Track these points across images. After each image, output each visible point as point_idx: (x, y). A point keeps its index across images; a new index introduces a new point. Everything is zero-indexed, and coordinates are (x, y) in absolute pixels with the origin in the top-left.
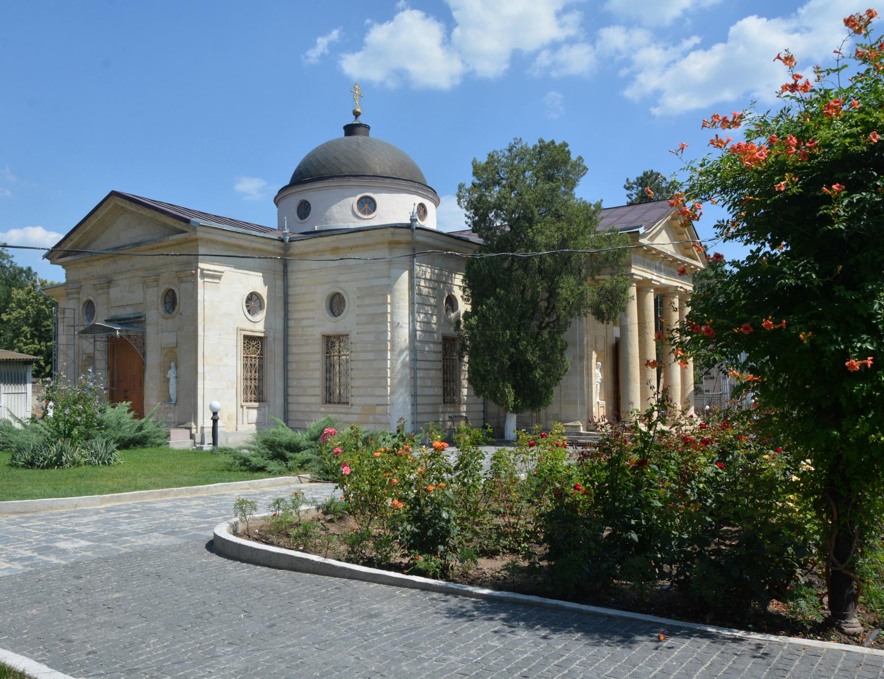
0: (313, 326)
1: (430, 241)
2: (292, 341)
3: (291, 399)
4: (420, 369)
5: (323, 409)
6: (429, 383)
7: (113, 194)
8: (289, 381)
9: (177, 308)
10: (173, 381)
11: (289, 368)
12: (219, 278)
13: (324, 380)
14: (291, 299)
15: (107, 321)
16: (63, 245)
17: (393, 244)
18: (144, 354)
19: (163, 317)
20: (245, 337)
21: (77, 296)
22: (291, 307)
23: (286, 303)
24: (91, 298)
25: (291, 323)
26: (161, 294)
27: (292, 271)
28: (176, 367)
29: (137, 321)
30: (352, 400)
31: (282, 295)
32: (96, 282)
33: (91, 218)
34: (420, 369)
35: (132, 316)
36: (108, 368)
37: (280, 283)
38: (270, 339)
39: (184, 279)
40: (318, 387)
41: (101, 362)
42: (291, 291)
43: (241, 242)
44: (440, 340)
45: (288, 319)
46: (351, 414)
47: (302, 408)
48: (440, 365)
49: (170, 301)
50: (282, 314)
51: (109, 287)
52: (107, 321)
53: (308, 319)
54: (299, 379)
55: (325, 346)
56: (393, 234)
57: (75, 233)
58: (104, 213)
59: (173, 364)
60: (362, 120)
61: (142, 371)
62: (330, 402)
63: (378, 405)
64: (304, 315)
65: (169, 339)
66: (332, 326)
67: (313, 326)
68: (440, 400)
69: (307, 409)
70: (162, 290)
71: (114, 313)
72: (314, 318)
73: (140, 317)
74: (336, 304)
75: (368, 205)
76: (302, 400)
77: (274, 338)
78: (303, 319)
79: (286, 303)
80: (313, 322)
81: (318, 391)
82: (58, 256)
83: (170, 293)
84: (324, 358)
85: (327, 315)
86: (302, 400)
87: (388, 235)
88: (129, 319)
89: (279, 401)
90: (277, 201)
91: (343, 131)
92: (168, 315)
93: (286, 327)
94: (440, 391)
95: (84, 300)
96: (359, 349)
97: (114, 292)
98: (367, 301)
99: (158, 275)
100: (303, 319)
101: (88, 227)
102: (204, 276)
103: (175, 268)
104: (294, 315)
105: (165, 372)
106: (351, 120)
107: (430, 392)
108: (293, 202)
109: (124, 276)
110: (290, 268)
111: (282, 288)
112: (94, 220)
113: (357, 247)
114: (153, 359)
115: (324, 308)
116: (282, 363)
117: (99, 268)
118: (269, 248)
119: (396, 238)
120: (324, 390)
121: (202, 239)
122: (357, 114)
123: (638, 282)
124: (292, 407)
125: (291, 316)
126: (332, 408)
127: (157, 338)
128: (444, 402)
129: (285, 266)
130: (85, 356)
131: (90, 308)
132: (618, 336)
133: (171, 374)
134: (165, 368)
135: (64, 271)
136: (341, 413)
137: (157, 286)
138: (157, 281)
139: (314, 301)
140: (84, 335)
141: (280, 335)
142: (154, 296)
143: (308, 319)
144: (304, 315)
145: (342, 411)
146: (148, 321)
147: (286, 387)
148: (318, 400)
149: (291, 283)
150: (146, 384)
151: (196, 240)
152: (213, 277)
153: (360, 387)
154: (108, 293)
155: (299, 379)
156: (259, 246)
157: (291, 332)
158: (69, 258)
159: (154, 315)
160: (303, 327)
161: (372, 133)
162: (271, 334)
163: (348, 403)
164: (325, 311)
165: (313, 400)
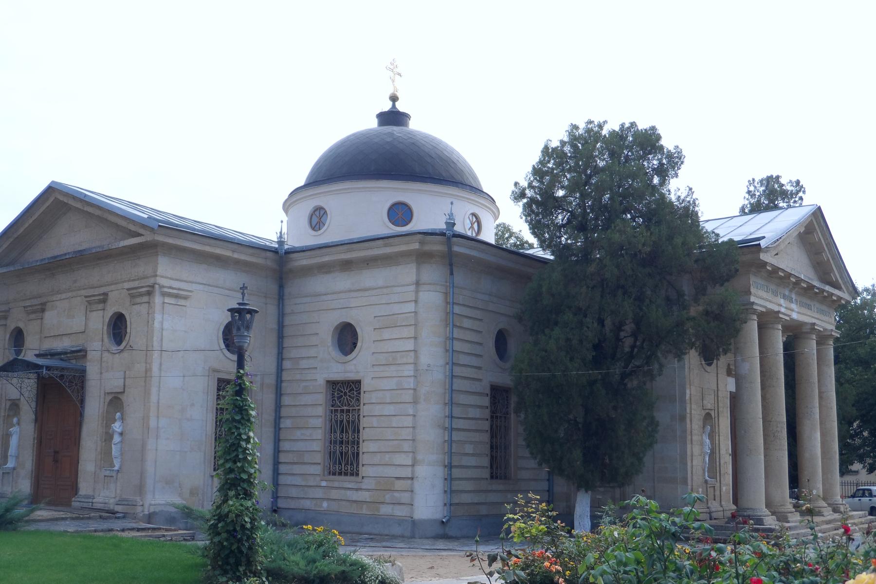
1: (474, 253)
3: (283, 469)
4: (458, 430)
5: (324, 484)
6: (469, 449)
8: (282, 444)
10: (116, 438)
12: (185, 298)
13: (327, 444)
14: (287, 331)
15: (37, 356)
22: (287, 343)
23: (281, 337)
24: (21, 325)
25: (287, 364)
26: (107, 320)
30: (363, 471)
31: (275, 326)
34: (458, 430)
36: (36, 420)
41: (28, 412)
42: (288, 321)
43: (218, 251)
44: (488, 391)
47: (298, 481)
48: (486, 425)
50: (275, 351)
51: (43, 311)
52: (37, 356)
55: (329, 397)
56: (422, 243)
60: (401, 107)
62: (334, 474)
65: (114, 382)
66: (341, 369)
68: (486, 474)
69: (303, 483)
70: (109, 313)
74: (347, 338)
75: (400, 213)
77: (262, 385)
79: (281, 337)
81: (318, 458)
85: (335, 353)
86: (297, 469)
88: (66, 353)
90: (287, 206)
93: (280, 370)
94: (486, 461)
95: (13, 327)
98: (387, 334)
102: (164, 294)
104: (290, 354)
106: (387, 106)
107: (472, 461)
108: (306, 207)
109: (64, 296)
110: (287, 290)
114: (94, 407)
115: (330, 344)
118: (260, 261)
119: (427, 248)
120: (327, 456)
121: (164, 244)
122: (394, 99)
123: (761, 315)
125: (286, 354)
128: (492, 477)
129: (281, 287)
130: (8, 403)
132: (734, 390)
138: (104, 301)
141: (271, 380)
142: (99, 321)
145: (350, 486)
148: (317, 470)
149: (288, 310)
152: (177, 296)
156: (243, 257)
157: (285, 376)
164: (331, 349)
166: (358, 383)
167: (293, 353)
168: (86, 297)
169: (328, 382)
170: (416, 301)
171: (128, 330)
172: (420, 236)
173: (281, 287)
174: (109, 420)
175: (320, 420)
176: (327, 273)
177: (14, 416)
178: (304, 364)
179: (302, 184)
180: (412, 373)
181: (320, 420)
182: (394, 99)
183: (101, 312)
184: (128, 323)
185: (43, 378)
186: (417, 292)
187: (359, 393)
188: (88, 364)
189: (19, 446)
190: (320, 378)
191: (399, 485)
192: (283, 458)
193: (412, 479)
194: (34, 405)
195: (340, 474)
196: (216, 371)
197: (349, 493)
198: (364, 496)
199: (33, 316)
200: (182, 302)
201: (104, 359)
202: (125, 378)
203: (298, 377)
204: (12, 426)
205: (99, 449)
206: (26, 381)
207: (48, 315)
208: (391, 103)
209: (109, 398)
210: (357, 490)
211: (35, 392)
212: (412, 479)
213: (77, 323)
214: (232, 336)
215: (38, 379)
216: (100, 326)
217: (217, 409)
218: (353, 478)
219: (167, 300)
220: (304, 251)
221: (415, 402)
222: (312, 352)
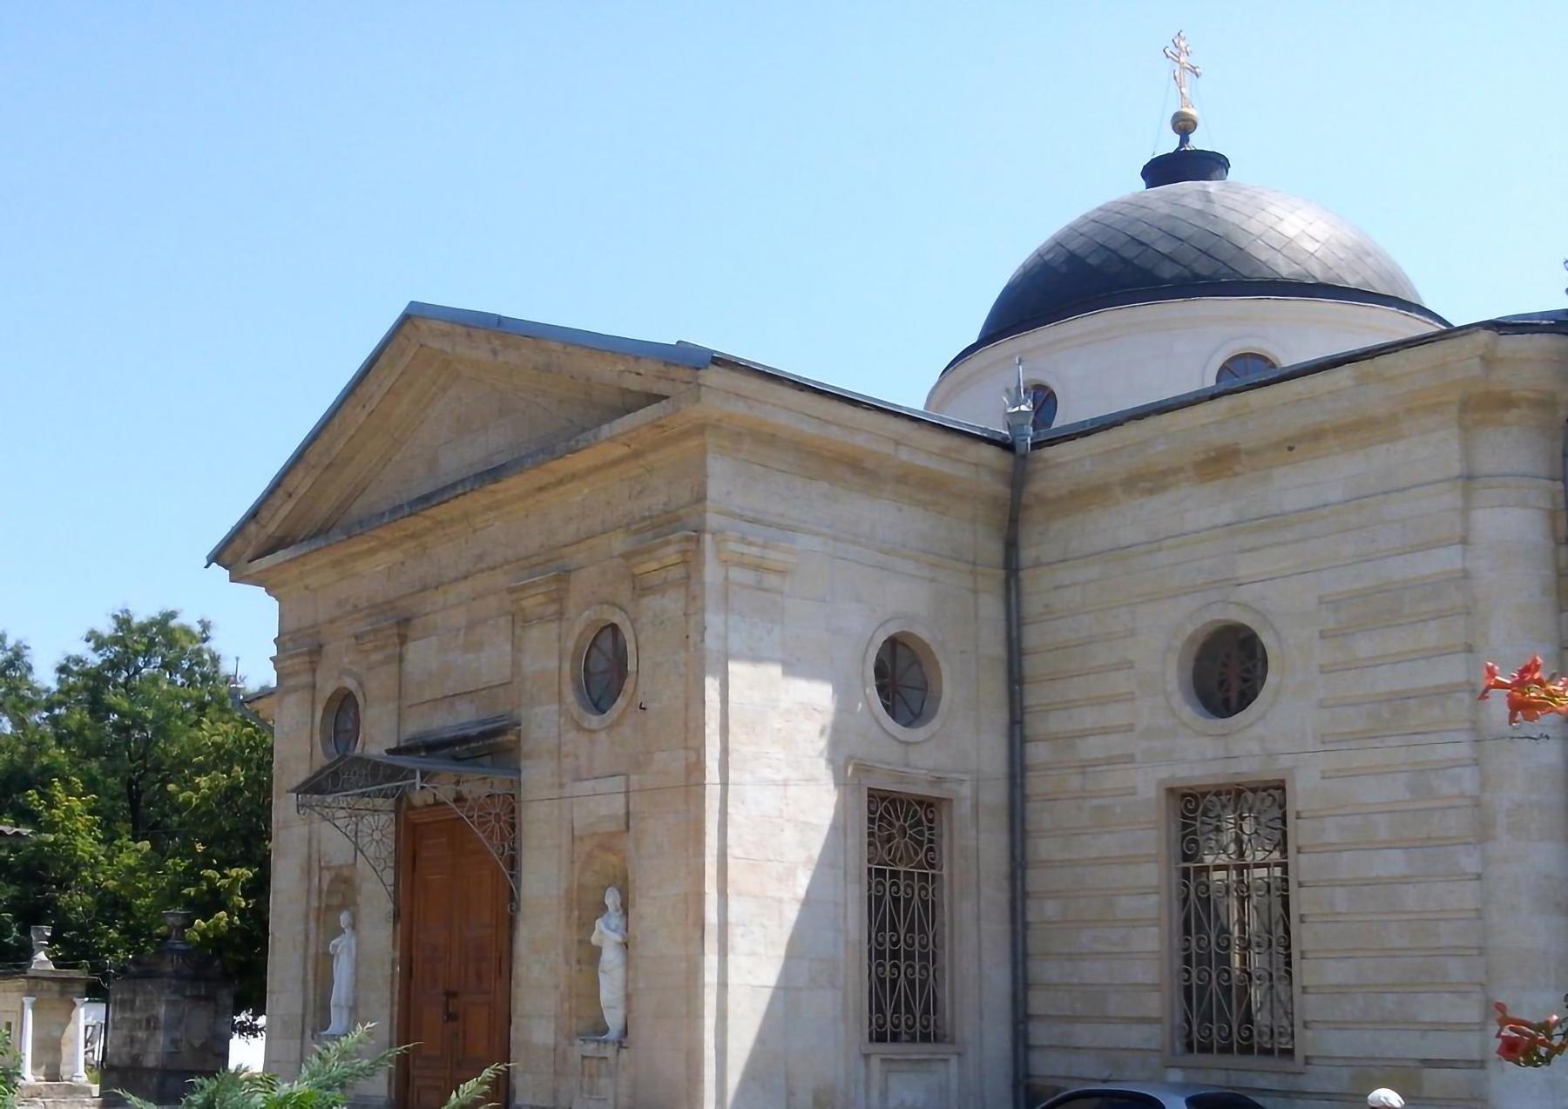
0: (1131, 758)
2: (1039, 816)
9: (629, 685)
11: (1031, 917)
13: (1178, 963)
14: (1032, 665)
17: (1482, 407)
19: (579, 728)
22: (1034, 696)
23: (1015, 679)
24: (350, 684)
25: (1037, 753)
26: (570, 644)
27: (1037, 564)
28: (625, 907)
29: (489, 746)
31: (998, 650)
32: (363, 627)
37: (992, 607)
38: (963, 809)
40: (1156, 987)
41: (376, 896)
42: (1032, 637)
45: (1024, 740)
50: (1002, 717)
51: (403, 640)
52: (389, 752)
53: (1105, 731)
54: (1070, 957)
55: (1176, 833)
59: (612, 899)
61: (509, 924)
62: (1206, 1049)
64: (1088, 718)
65: (600, 804)
66: (1208, 751)
67: (1131, 758)
71: (415, 726)
72: (1130, 728)
73: (501, 731)
77: (976, 807)
78: (1085, 734)
79: (1015, 679)
81: (1153, 1004)
83: (606, 643)
84: (1176, 877)
88: (465, 740)
96: (1332, 836)
97: (421, 655)
99: (564, 575)
100: (1085, 734)
104: (1046, 725)
105: (587, 926)
110: (1027, 554)
111: (1002, 625)
113: (1316, 435)
114: (543, 879)
116: (1003, 898)
125: (1033, 725)
127: (561, 804)
129: (1011, 546)
130: (327, 876)
131: (343, 712)
133: (606, 934)
137: (560, 616)
138: (559, 598)
139: (1130, 665)
143: (1105, 731)
144: (1088, 718)
146: (526, 747)
147: (1021, 986)
149: (1032, 605)
151: (700, 429)
153: (1341, 990)
154: (401, 659)
155: (1070, 957)
157: (1036, 784)
158: (281, 556)
159: (546, 722)
160: (1084, 767)
162: (966, 790)
163: (1288, 1053)
164: (1177, 699)
165: (1135, 1036)
167: (1055, 723)
169: (1171, 791)
170: (1464, 541)
171: (631, 667)
172: (1485, 336)
173: (1011, 546)
174: (586, 910)
175: (1153, 899)
177: (343, 907)
178: (1092, 748)
181: (1153, 899)
183: (553, 626)
184: (631, 647)
185: (411, 807)
186: (1466, 511)
189: (357, 983)
194: (389, 876)
195: (1226, 1050)
196: (862, 768)
199: (376, 657)
200: (772, 580)
201: (564, 749)
203: (1074, 782)
204: (339, 931)
206: (369, 819)
211: (390, 842)
213: (489, 661)
215: (397, 811)
216: (553, 664)
219: (736, 574)
220: (1086, 434)
221: (1483, 833)
222: (1116, 714)
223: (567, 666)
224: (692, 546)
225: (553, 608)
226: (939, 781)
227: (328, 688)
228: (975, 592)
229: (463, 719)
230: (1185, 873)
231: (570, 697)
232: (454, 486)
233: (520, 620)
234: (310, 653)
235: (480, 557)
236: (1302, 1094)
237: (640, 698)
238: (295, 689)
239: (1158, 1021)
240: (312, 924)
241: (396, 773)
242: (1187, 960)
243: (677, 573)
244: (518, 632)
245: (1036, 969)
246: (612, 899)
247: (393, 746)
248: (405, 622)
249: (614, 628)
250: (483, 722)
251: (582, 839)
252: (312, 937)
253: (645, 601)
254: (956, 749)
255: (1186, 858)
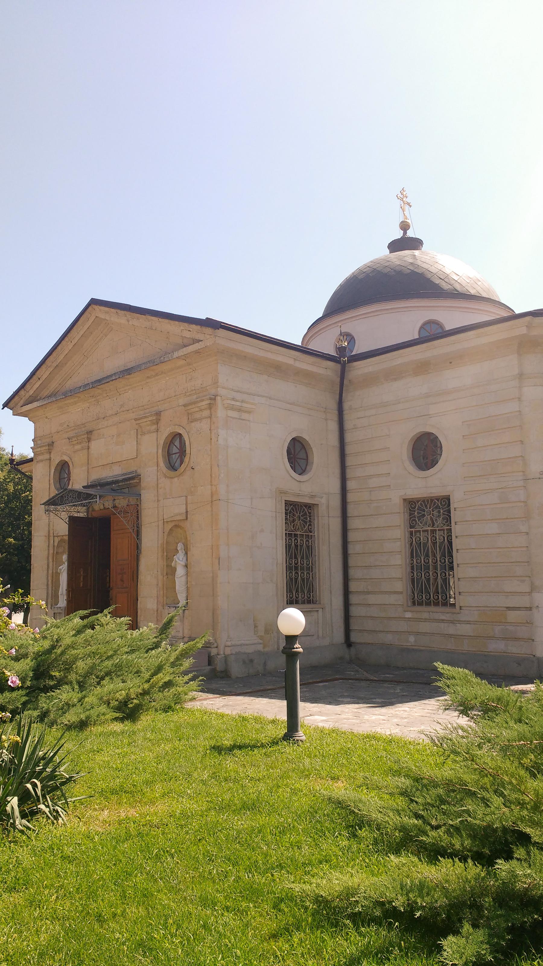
3: (353, 599)
5: (408, 615)
7: (94, 302)
9: (186, 459)
10: (180, 571)
11: (350, 551)
13: (409, 569)
14: (349, 449)
16: (28, 386)
18: (138, 534)
19: (166, 477)
20: (288, 503)
21: (47, 456)
22: (349, 461)
24: (66, 458)
25: (351, 485)
26: (162, 442)
32: (71, 434)
33: (63, 343)
35: (121, 478)
37: (333, 426)
39: (197, 416)
42: (349, 437)
46: (460, 622)
49: (175, 452)
50: (337, 471)
51: (89, 440)
52: (84, 487)
53: (379, 475)
55: (407, 516)
57: (44, 367)
58: (82, 333)
59: (180, 546)
60: (410, 234)
62: (420, 604)
63: (509, 608)
65: (174, 509)
74: (426, 451)
76: (372, 599)
77: (328, 507)
80: (389, 482)
81: (399, 586)
82: (22, 402)
83: (177, 443)
84: (407, 535)
86: (372, 599)
87: (519, 329)
89: (338, 601)
91: (388, 251)
92: (172, 473)
97: (97, 446)
99: (158, 414)
100: (370, 477)
101: (59, 356)
103: (181, 401)
106: (398, 234)
112: (67, 346)
114: (151, 539)
117: (76, 413)
122: (405, 226)
124: (354, 611)
126: (425, 612)
130: (57, 540)
131: (63, 469)
133: (179, 560)
134: (169, 554)
135: (31, 425)
136: (443, 621)
138: (157, 422)
140: (52, 507)
145: (443, 617)
146: (143, 484)
148: (401, 599)
149: (348, 425)
150: (141, 577)
157: (350, 497)
159: (152, 473)
161: (424, 248)
162: (324, 501)
165: (392, 599)
166: (446, 500)
168: (136, 420)
169: (405, 500)
171: (188, 451)
175: (398, 544)
176: (395, 380)
179: (321, 315)
180: (521, 483)
182: (405, 226)
183: (155, 434)
185: (93, 510)
187: (449, 511)
188: (143, 492)
190: (396, 498)
191: (512, 616)
192: (353, 586)
193: (530, 609)
195: (428, 604)
196: (282, 492)
197: (442, 625)
198: (464, 629)
199: (78, 447)
200: (245, 416)
201: (160, 486)
202: (186, 504)
205: (160, 584)
207: (93, 445)
208: (402, 232)
209: (170, 526)
210: (452, 622)
212: (530, 609)
213: (127, 450)
214: (298, 454)
217: (286, 534)
218: (448, 609)
219: (231, 413)
223: (160, 451)
224: (212, 402)
225: (154, 427)
226: (313, 497)
227: (56, 460)
228: (326, 420)
229: (116, 473)
230: (411, 533)
231: (162, 464)
232: (111, 376)
233: (140, 433)
234: (49, 445)
235: (122, 406)
236: (460, 622)
237: (192, 464)
238: (42, 461)
239: (401, 593)
240: (51, 560)
241: (89, 496)
242: (412, 568)
243: (206, 413)
244: (139, 437)
245: (352, 572)
246: (180, 546)
247: (86, 484)
248: (90, 432)
249: (180, 435)
250: (125, 474)
251: (167, 522)
252: (51, 565)
253: (193, 424)
254: (319, 484)
255: (411, 527)
